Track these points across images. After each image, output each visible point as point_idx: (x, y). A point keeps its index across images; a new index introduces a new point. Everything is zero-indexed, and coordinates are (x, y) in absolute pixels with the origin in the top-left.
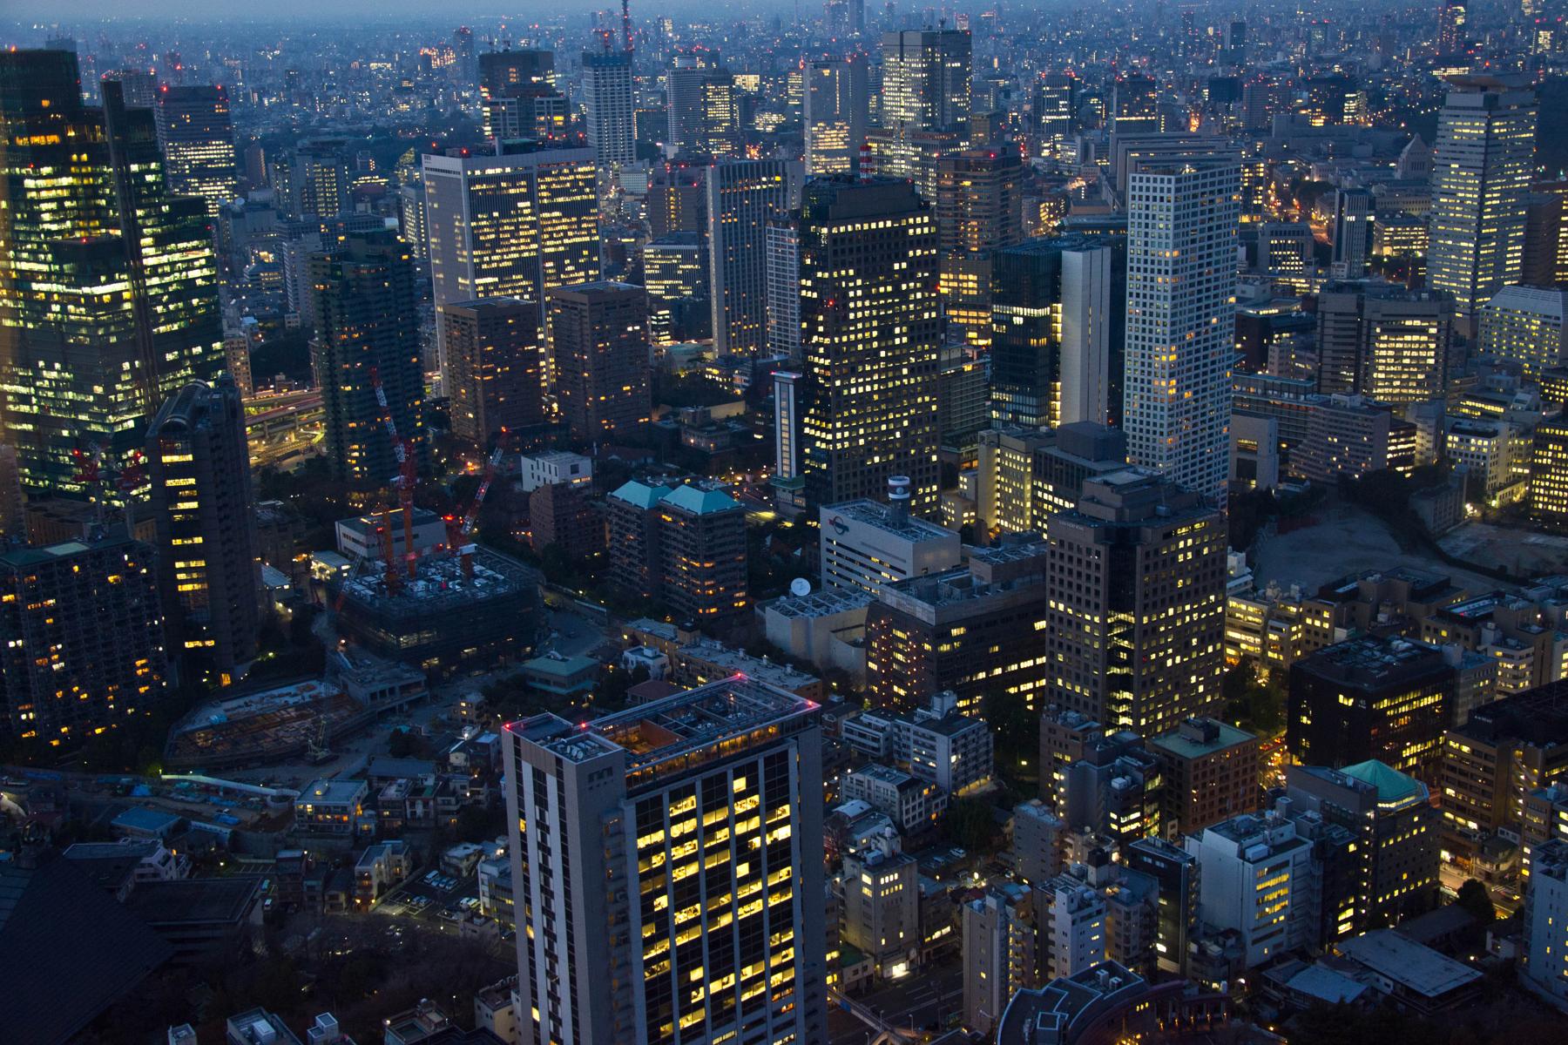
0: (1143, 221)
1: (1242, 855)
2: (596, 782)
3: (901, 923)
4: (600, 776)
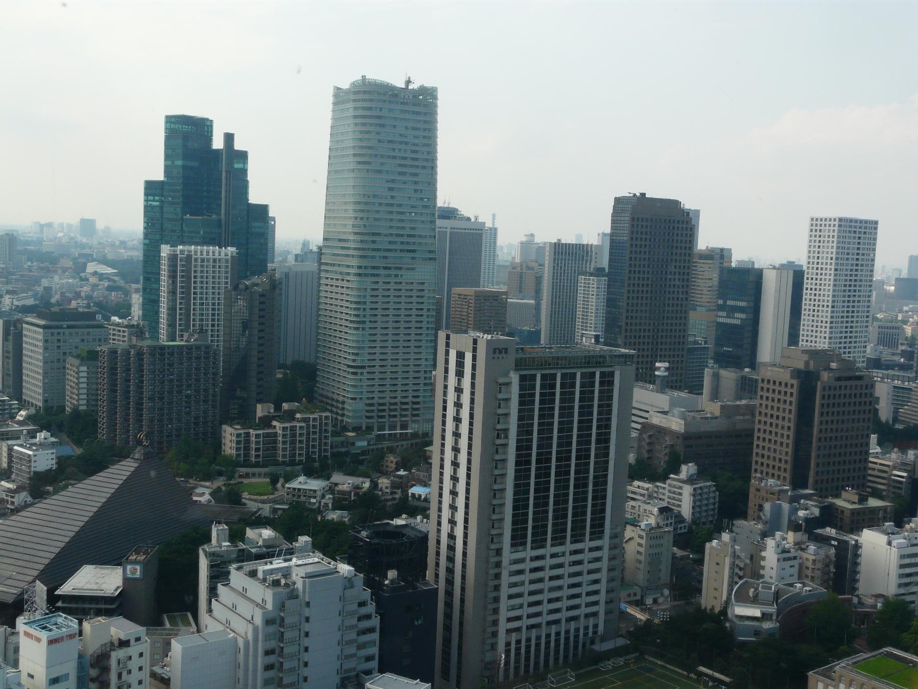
0: (817, 244)
1: (889, 543)
2: (497, 355)
3: (660, 570)
4: (500, 352)
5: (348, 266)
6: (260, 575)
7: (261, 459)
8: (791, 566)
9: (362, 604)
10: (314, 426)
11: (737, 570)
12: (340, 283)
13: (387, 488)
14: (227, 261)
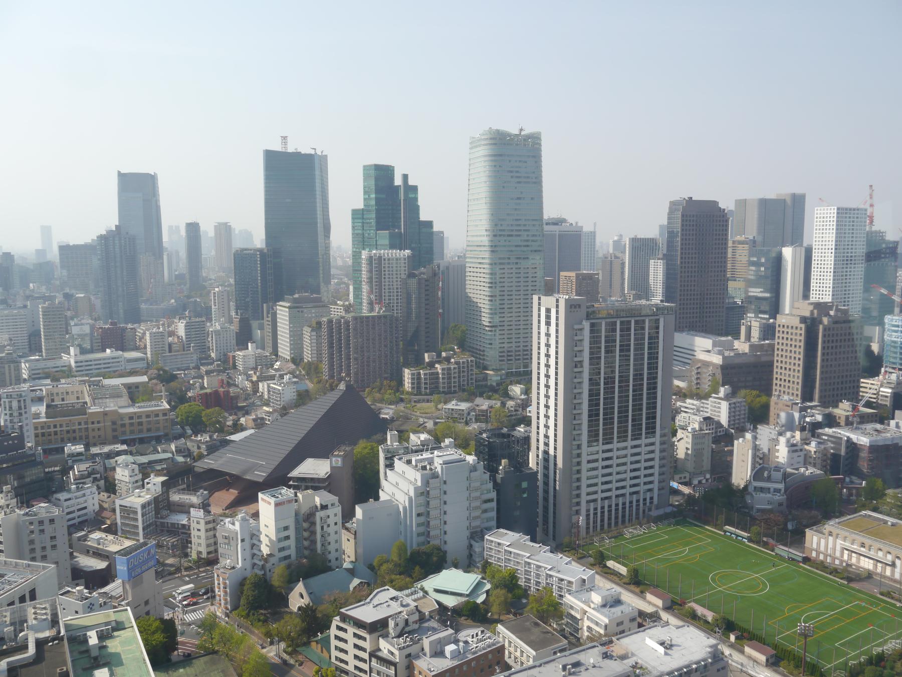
2: (573, 310)
4: (575, 307)
5: (483, 258)
6: (414, 463)
7: (428, 391)
8: (798, 456)
10: (463, 367)
11: (758, 459)
12: (478, 270)
13: (512, 407)
14: (405, 259)
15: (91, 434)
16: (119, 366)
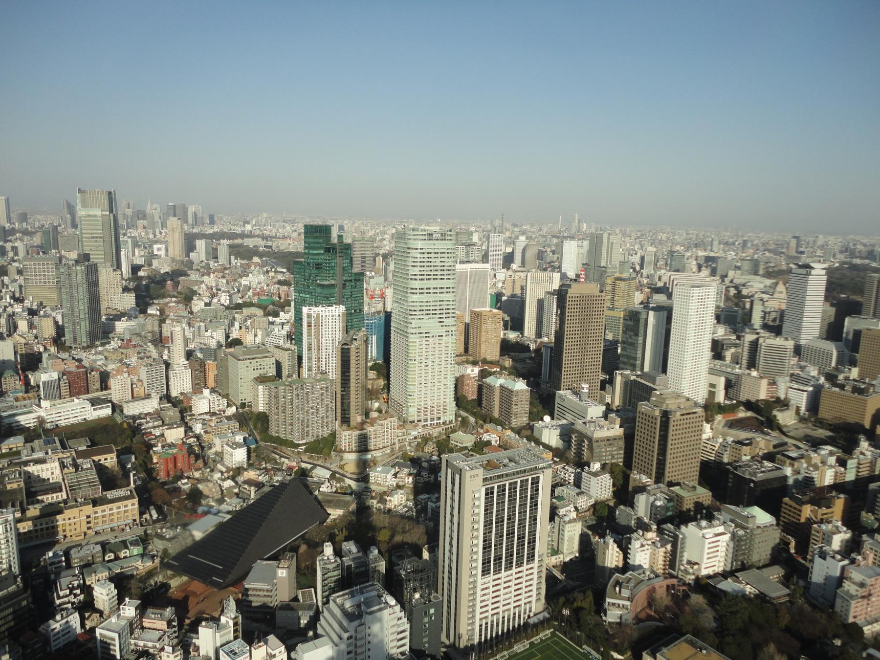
9: (400, 619)
15: (68, 528)
16: (86, 415)
